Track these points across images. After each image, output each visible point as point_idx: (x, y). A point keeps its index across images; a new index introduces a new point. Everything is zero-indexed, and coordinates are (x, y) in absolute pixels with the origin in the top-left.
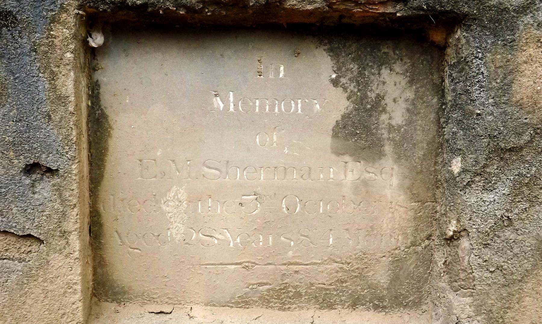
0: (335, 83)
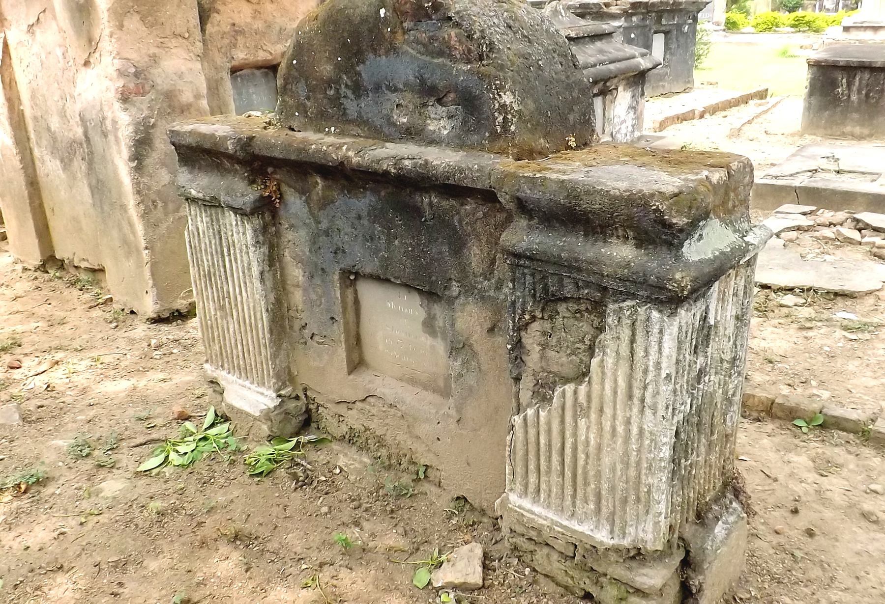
0: (421, 305)
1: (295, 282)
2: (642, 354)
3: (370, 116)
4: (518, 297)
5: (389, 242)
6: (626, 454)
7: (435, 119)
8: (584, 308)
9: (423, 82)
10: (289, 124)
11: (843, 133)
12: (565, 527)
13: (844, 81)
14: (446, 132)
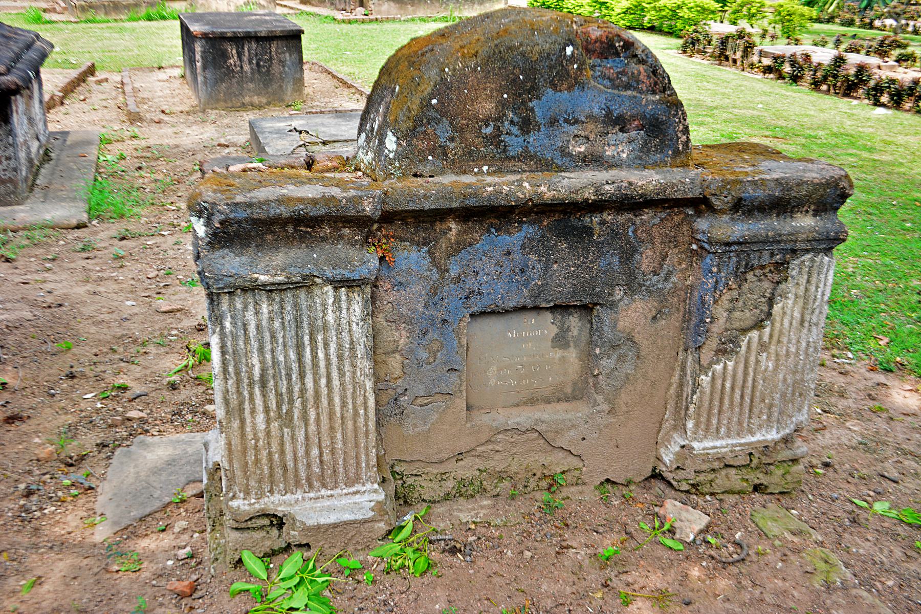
1: (392, 347)
2: (814, 288)
3: (539, 149)
4: (721, 278)
5: (546, 269)
6: (797, 364)
7: (614, 145)
8: (768, 271)
9: (609, 113)
10: (414, 170)
11: (243, 104)
12: (741, 445)
13: (234, 52)
14: (625, 155)
